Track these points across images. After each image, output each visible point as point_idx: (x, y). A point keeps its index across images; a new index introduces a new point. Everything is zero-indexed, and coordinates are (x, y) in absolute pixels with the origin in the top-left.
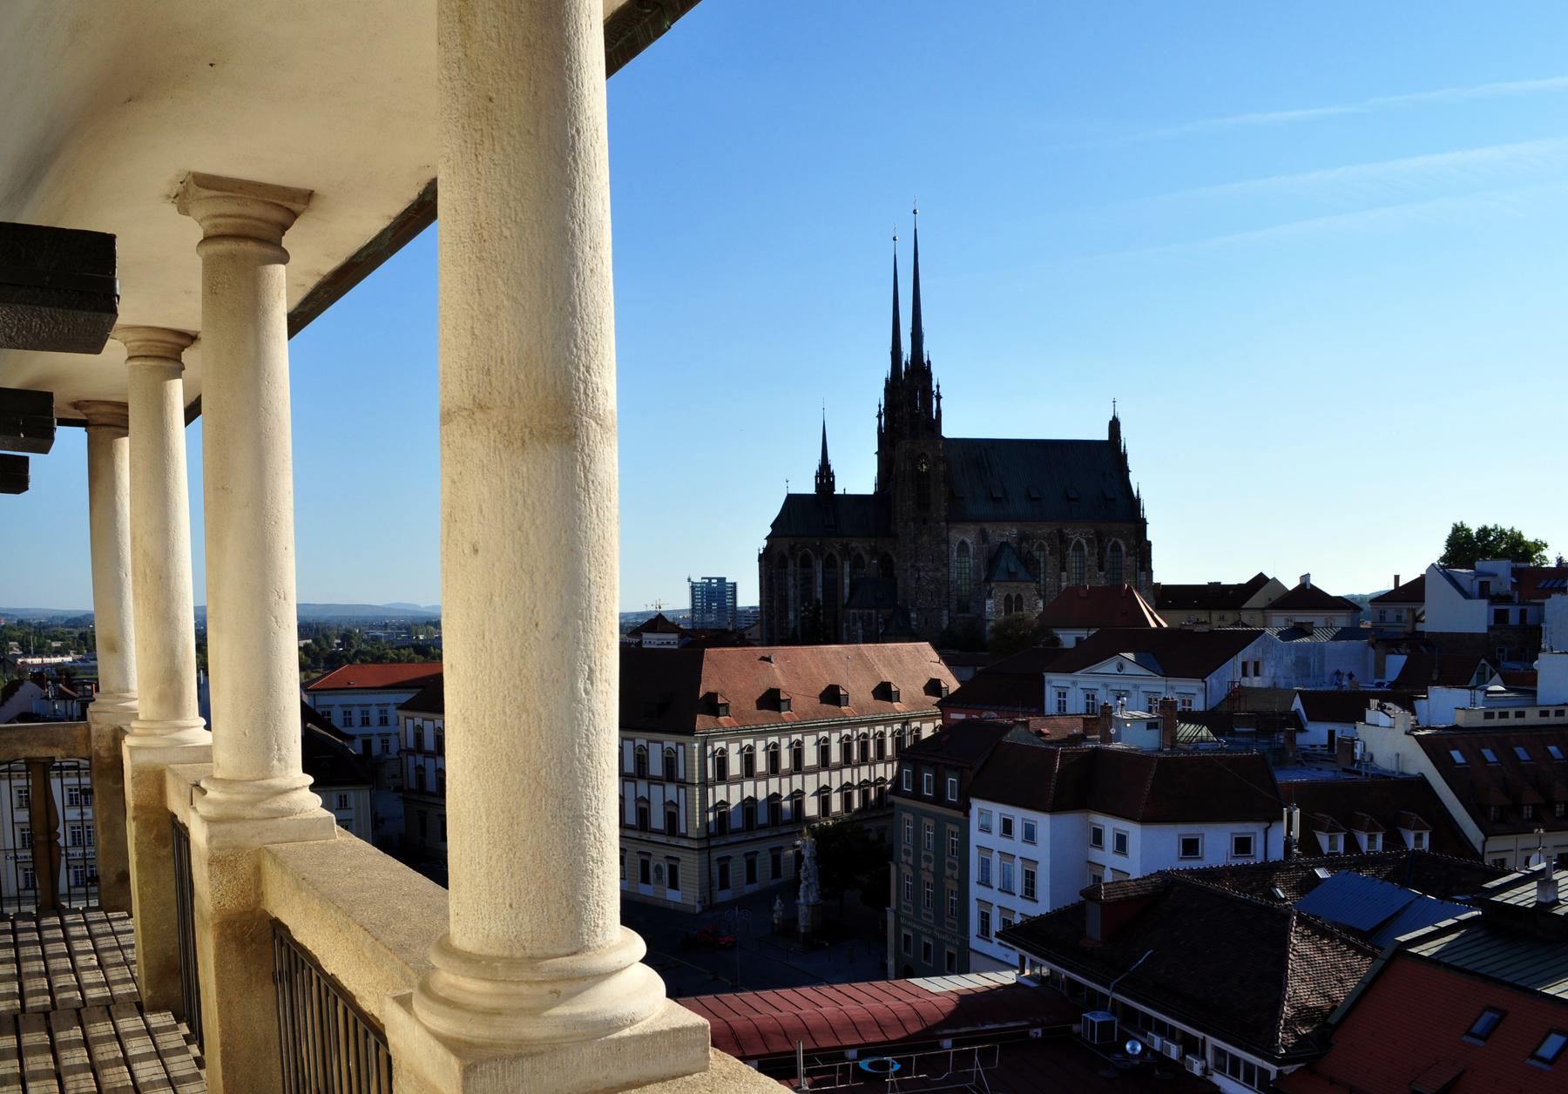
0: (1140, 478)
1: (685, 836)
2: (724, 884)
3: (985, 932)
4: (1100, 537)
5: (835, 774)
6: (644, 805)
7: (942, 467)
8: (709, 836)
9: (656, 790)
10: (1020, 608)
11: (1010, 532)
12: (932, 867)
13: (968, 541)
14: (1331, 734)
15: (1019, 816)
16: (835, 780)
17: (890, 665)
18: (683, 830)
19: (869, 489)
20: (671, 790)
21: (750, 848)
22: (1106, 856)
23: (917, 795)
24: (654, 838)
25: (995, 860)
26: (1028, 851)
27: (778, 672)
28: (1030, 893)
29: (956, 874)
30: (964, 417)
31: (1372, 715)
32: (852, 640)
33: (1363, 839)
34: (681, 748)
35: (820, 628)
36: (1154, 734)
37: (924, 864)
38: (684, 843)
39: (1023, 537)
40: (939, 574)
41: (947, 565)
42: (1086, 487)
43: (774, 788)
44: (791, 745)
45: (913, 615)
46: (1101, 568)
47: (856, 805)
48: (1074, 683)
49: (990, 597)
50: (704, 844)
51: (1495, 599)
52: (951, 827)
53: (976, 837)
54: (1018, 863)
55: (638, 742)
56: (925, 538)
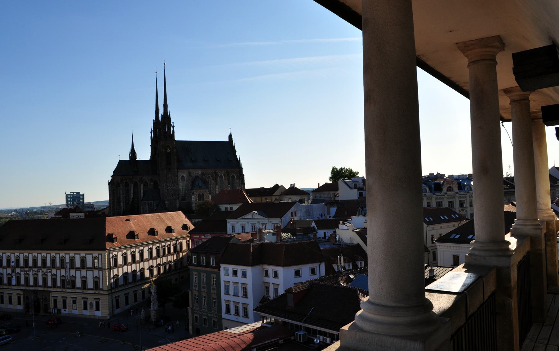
0: (240, 154)
1: (102, 290)
2: (118, 307)
3: (228, 311)
4: (228, 173)
5: (155, 261)
6: (84, 279)
7: (175, 151)
8: (112, 289)
9: (90, 273)
10: (203, 199)
11: (199, 172)
12: (206, 290)
13: (185, 176)
14: (325, 233)
15: (239, 268)
16: (154, 263)
17: (169, 220)
18: (101, 287)
19: (148, 158)
20: (96, 273)
21: (126, 292)
22: (271, 279)
23: (199, 264)
24: (78, 291)
25: (231, 285)
26: (244, 280)
27: (132, 225)
28: (245, 295)
29: (215, 292)
30: (182, 134)
31: (340, 226)
32: (145, 212)
33: (359, 264)
34: (100, 256)
35: (134, 209)
36: (275, 236)
37: (202, 290)
38: (102, 292)
39: (203, 174)
40: (175, 188)
41: (178, 184)
42: (222, 156)
43: (134, 268)
44: (139, 251)
45: (166, 202)
46: (229, 184)
47: (162, 272)
48: (237, 222)
49: (193, 195)
50: (110, 292)
51: (359, 189)
52: (213, 275)
53: (223, 278)
54: (240, 285)
55: (82, 255)
56: (170, 175)
